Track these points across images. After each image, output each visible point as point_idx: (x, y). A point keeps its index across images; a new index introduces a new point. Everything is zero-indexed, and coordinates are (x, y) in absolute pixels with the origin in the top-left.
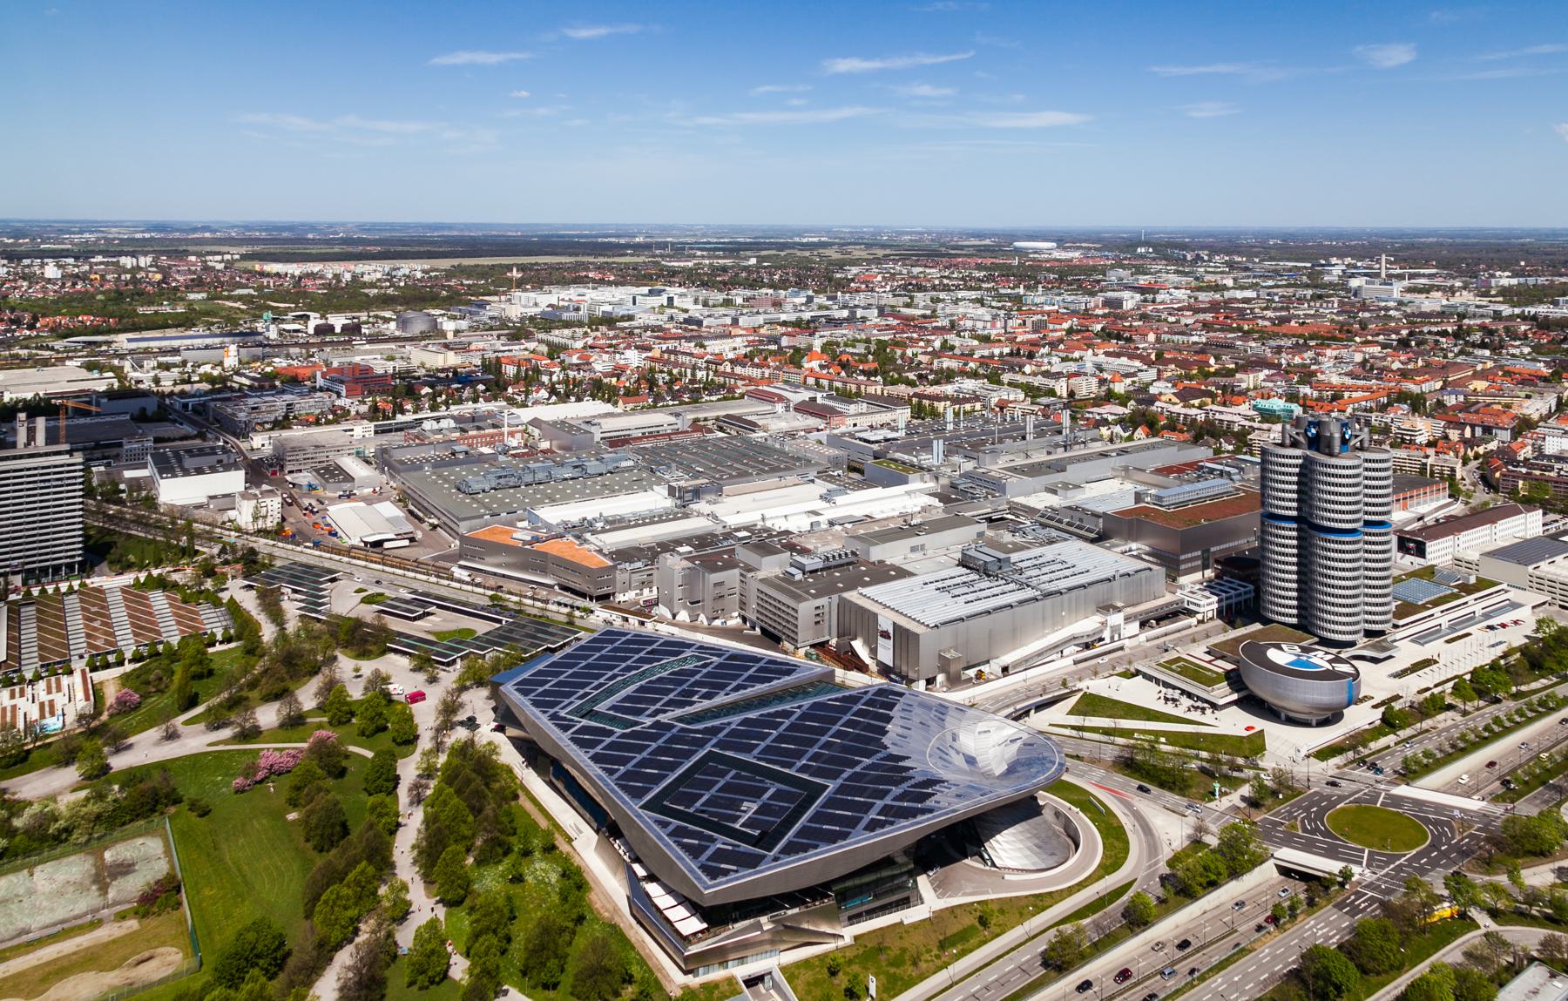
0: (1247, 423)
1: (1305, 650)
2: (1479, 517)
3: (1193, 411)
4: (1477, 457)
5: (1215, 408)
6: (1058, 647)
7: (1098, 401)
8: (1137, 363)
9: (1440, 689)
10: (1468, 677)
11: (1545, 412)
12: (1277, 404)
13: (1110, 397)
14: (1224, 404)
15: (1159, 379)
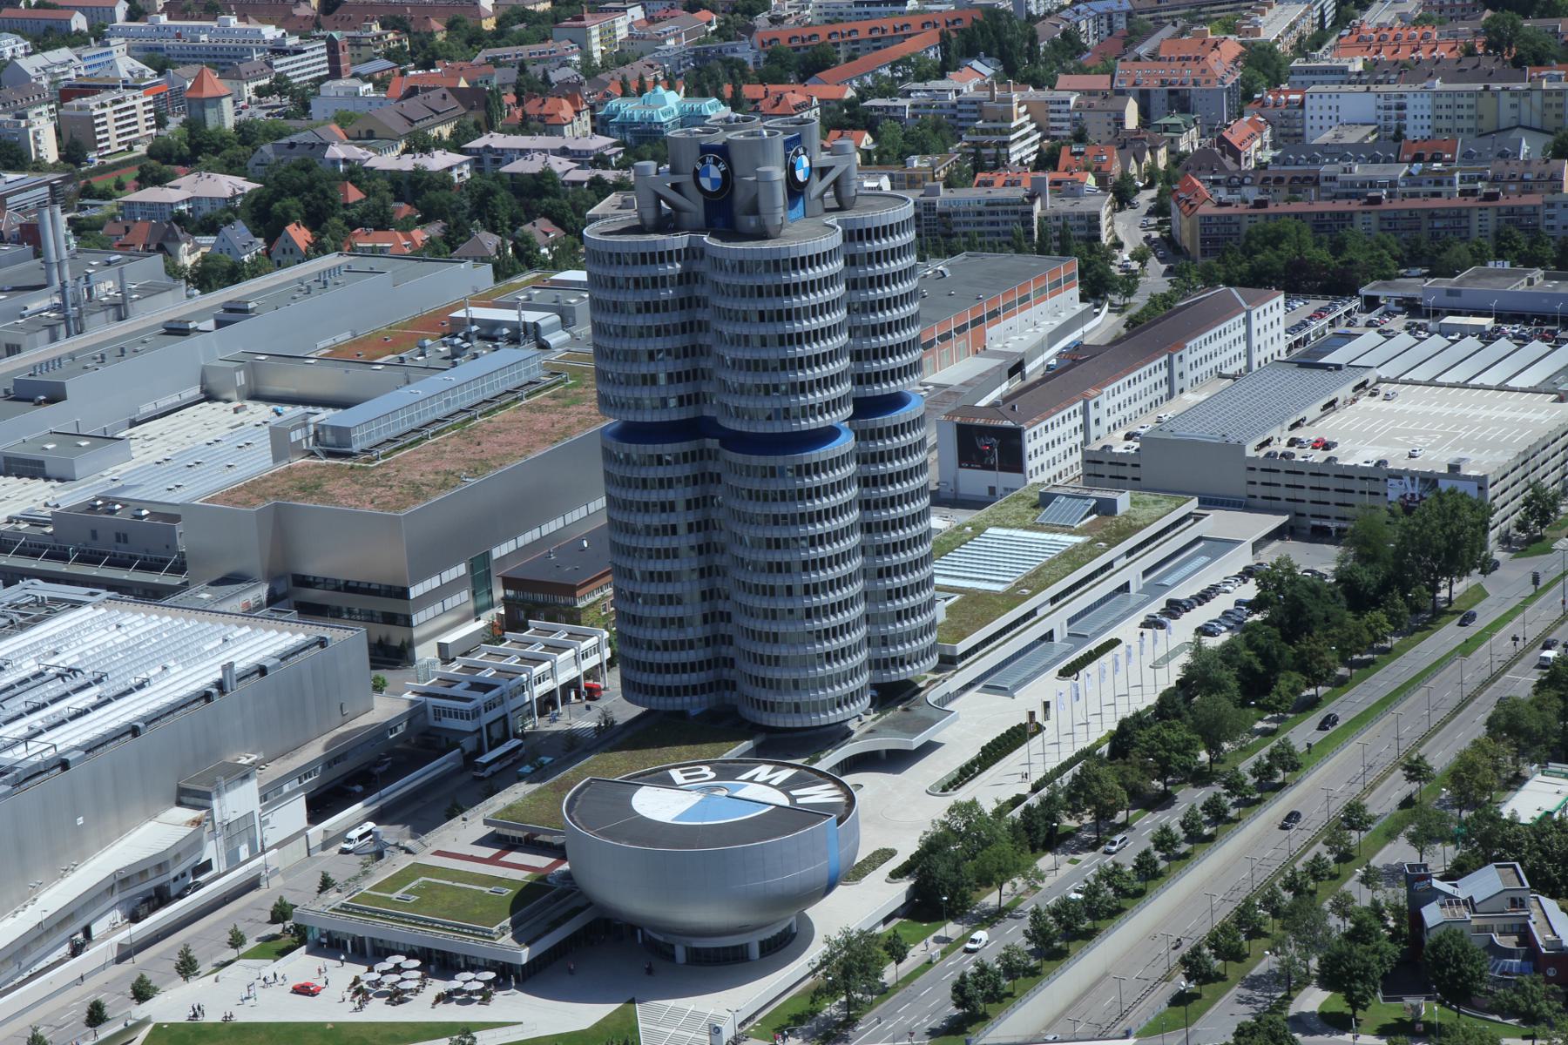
0: (585, 175)
1: (727, 771)
2: (1153, 334)
3: (438, 161)
4: (1152, 177)
5: (497, 140)
6: (72, 932)
7: (162, 162)
8: (270, 32)
9: (1044, 792)
10: (1105, 748)
11: (1308, 28)
12: (669, 103)
13: (198, 148)
14: (524, 127)
15: (335, 73)
